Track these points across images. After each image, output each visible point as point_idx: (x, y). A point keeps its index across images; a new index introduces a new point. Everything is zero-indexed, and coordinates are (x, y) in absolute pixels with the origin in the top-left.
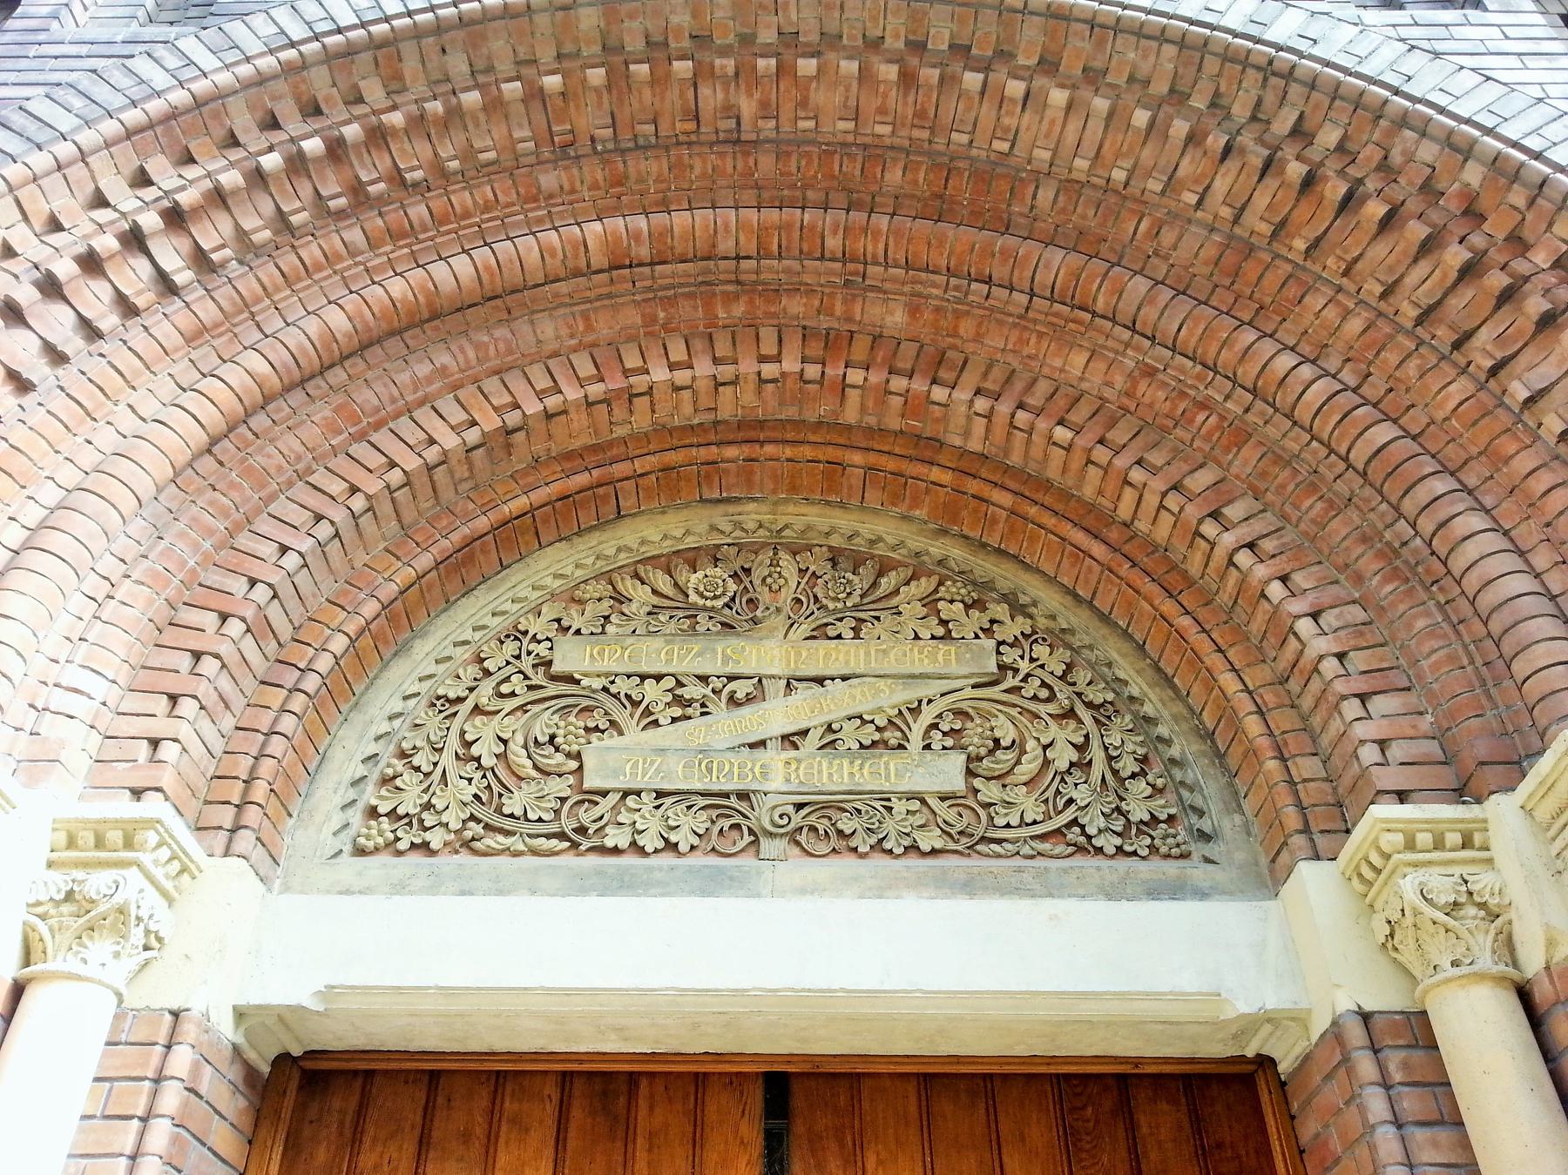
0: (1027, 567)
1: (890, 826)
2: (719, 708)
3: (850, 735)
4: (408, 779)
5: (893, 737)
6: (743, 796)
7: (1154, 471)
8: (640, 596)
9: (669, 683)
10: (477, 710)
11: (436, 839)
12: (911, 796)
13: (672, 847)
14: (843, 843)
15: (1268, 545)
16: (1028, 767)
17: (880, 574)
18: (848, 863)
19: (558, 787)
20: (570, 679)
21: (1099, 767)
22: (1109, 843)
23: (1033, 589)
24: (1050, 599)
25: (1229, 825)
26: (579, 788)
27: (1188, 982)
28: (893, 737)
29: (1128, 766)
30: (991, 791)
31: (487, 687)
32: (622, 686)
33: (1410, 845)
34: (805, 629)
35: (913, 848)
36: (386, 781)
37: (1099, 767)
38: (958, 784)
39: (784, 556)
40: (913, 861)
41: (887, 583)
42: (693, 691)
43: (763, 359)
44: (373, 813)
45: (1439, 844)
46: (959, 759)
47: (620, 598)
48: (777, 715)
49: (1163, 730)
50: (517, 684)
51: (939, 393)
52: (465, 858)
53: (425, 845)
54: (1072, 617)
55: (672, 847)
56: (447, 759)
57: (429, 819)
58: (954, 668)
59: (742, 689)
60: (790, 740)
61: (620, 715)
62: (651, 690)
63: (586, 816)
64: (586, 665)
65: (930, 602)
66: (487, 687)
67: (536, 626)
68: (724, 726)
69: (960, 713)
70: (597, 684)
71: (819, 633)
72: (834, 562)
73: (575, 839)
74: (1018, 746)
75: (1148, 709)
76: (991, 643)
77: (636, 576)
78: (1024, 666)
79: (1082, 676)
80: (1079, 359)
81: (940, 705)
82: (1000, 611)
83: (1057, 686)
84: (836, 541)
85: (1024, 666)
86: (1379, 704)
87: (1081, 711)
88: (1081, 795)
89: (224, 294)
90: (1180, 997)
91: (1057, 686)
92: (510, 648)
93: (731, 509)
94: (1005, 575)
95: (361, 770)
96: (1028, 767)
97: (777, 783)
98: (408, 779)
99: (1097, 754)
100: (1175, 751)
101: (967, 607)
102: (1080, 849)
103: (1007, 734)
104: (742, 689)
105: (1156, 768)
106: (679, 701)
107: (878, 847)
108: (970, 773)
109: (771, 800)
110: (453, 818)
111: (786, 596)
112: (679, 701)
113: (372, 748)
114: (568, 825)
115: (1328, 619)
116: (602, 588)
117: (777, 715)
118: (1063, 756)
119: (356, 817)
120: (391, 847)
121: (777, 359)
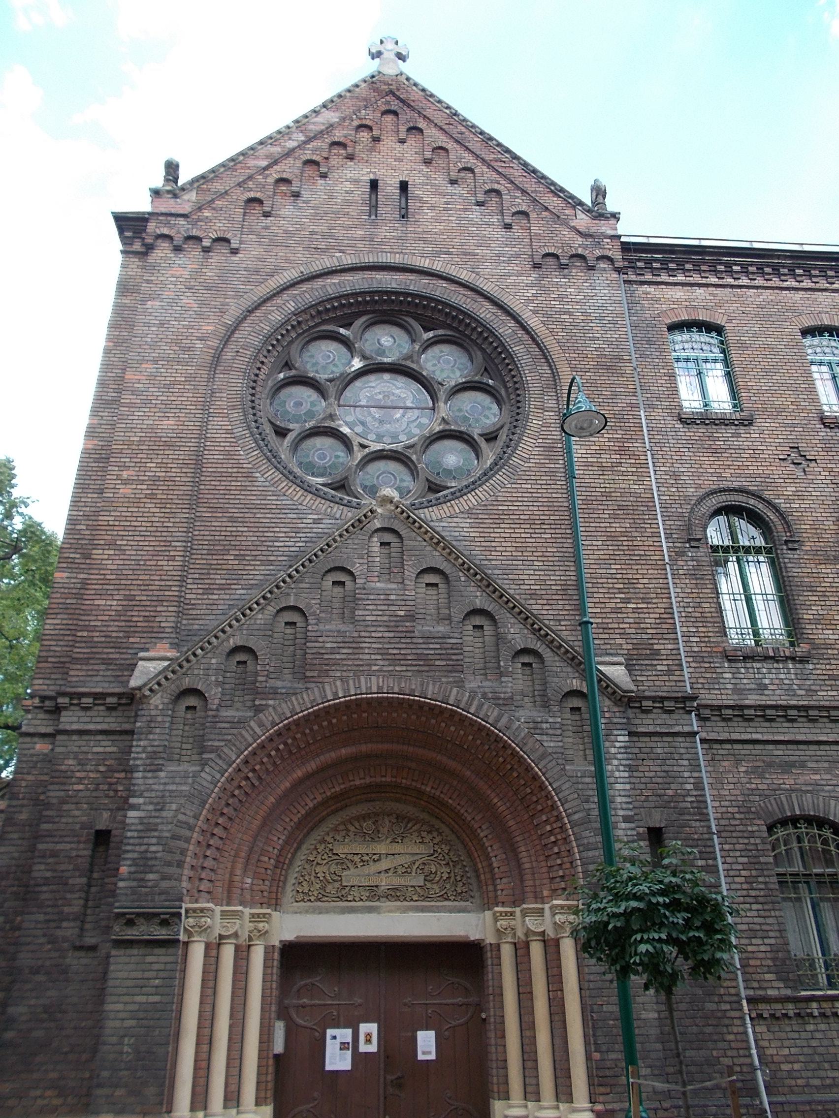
0: (443, 823)
1: (408, 894)
2: (371, 863)
3: (400, 870)
4: (305, 884)
5: (409, 870)
6: (376, 886)
7: (469, 814)
8: (352, 829)
9: (360, 856)
10: (318, 864)
11: (312, 898)
12: (412, 887)
13: (362, 900)
14: (398, 898)
15: (490, 837)
16: (437, 879)
17: (408, 822)
18: (399, 903)
19: (337, 885)
20: (337, 854)
21: (452, 879)
22: (452, 898)
23: (443, 828)
24: (447, 831)
25: (477, 894)
26: (341, 885)
27: (462, 933)
28: (409, 870)
29: (458, 878)
30: (429, 885)
31: (319, 857)
32: (349, 857)
33: (501, 915)
34: (389, 840)
35: (412, 900)
36: (299, 883)
37: (452, 879)
38: (422, 884)
39: (386, 817)
40: (412, 903)
41: (410, 825)
42: (366, 858)
43: (382, 776)
44: (298, 891)
45: (506, 915)
46: (422, 877)
47: (348, 830)
48: (384, 864)
49: (467, 869)
50: (325, 856)
51: (423, 787)
52: (319, 903)
53: (310, 900)
54: (452, 837)
55: (362, 900)
56: (313, 878)
57: (310, 893)
58: (423, 852)
59: (376, 857)
60: (386, 871)
61: (349, 865)
62: (356, 859)
63: (343, 892)
64: (341, 851)
65: (419, 831)
66: (319, 857)
67: (328, 839)
68: (373, 868)
69: (424, 864)
70: (343, 856)
71: (394, 841)
72: (397, 818)
73: (341, 898)
74: (436, 872)
75: (465, 863)
76: (432, 844)
77: (351, 823)
78: (439, 850)
79: (451, 854)
80: (455, 783)
81: (420, 861)
82: (435, 834)
83: (446, 857)
84: (398, 812)
85: (439, 850)
86: (504, 880)
87: (451, 864)
88: (448, 886)
89: (264, 783)
90: (461, 936)
91: (446, 857)
92: (323, 846)
93: (373, 803)
94: (437, 824)
95: (294, 881)
96: (437, 879)
97: (383, 883)
98: (305, 884)
99: (452, 875)
100: (469, 875)
101: (428, 833)
102: (446, 899)
103: (434, 870)
104: (376, 857)
105: (465, 878)
106: (362, 861)
107: (405, 900)
108: (425, 880)
109: (382, 888)
110: (315, 893)
111: (386, 829)
112: (362, 861)
113: (296, 875)
114: (340, 895)
115: (498, 858)
116: (342, 827)
117: (384, 864)
118: (445, 876)
119: (294, 892)
120: (303, 900)
121: (385, 777)
